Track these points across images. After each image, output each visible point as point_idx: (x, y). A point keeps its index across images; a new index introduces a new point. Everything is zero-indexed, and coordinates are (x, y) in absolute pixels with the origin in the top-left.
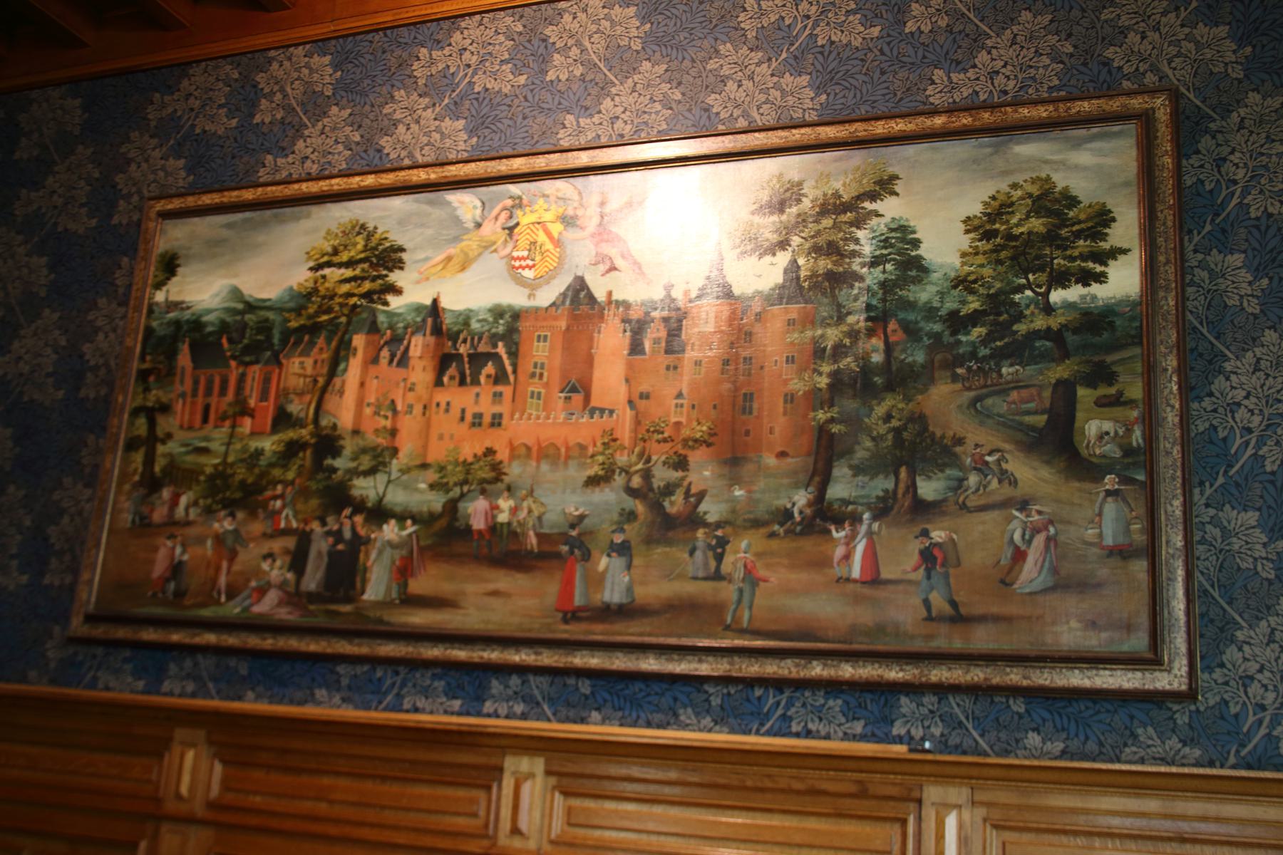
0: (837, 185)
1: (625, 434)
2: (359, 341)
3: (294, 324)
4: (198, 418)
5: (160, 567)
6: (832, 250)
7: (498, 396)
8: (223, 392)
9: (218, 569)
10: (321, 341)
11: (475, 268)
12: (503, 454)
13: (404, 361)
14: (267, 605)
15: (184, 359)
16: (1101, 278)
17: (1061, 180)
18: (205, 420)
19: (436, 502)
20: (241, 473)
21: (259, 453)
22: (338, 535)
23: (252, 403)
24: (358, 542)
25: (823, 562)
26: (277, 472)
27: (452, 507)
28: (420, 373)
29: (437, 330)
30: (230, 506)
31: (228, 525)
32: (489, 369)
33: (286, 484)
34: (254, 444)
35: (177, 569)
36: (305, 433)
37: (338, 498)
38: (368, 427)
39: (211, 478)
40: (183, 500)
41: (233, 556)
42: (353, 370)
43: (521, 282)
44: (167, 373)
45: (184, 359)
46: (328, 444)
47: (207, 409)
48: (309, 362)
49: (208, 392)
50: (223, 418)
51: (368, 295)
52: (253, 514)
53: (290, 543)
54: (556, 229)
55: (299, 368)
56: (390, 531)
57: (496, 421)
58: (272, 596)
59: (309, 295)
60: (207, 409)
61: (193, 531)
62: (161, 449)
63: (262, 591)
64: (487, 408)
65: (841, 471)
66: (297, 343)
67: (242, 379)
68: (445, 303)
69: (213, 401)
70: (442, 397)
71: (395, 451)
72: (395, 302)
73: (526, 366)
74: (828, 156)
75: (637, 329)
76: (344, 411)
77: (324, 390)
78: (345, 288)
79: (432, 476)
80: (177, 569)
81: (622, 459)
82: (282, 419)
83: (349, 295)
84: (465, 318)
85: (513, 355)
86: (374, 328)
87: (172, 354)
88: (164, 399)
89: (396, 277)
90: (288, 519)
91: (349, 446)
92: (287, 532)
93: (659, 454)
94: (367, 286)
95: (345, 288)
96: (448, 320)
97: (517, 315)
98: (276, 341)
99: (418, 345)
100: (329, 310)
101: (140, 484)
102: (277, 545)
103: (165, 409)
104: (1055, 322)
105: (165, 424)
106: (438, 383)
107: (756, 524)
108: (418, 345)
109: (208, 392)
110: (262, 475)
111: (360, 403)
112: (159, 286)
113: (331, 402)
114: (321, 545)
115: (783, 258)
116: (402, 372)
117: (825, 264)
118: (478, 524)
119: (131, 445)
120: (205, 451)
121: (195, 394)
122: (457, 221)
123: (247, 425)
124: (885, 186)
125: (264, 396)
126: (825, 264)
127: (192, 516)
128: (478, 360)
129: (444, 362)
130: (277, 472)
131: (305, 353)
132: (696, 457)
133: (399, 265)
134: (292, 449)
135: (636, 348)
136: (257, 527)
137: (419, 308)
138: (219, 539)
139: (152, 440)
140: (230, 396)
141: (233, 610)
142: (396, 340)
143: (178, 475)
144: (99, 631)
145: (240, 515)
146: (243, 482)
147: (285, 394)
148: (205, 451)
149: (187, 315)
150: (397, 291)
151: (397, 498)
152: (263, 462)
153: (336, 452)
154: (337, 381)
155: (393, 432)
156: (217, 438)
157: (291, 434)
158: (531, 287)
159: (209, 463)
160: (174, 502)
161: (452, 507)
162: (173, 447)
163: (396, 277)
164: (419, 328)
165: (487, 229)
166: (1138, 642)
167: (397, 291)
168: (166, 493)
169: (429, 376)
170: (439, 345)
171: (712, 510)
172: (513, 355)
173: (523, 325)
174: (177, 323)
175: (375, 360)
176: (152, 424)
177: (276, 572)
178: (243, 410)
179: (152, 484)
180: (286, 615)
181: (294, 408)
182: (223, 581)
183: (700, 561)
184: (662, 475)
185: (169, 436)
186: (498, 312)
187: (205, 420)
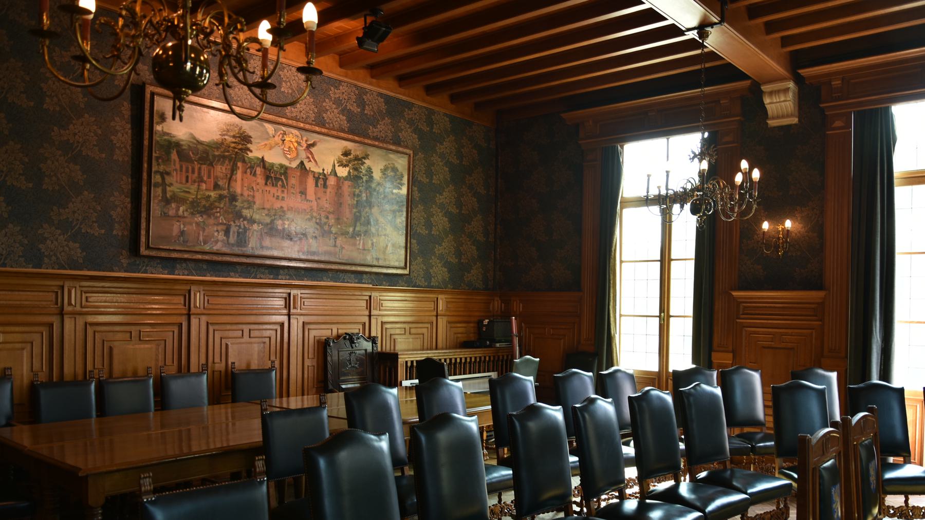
0: (358, 153)
1: (315, 208)
2: (239, 164)
3: (216, 153)
4: (184, 180)
5: (175, 232)
6: (356, 169)
7: (283, 191)
8: (193, 172)
9: (199, 234)
10: (227, 162)
11: (273, 150)
12: (285, 209)
13: (255, 175)
14: (218, 247)
15: (174, 156)
16: (400, 189)
17: (397, 165)
18: (187, 181)
19: (268, 220)
20: (204, 202)
21: (209, 196)
22: (239, 227)
23: (205, 178)
24: (245, 230)
25: (355, 245)
26: (217, 204)
27: (272, 222)
28: (260, 180)
29: (264, 167)
30: (201, 213)
31: (200, 219)
32: (280, 183)
33: (221, 208)
34: (207, 193)
35: (182, 233)
36: (225, 192)
37: (239, 215)
38: (246, 193)
39: (192, 203)
40: (181, 209)
41: (204, 230)
42: (239, 175)
43: (287, 158)
44: (167, 160)
45: (174, 156)
46: (233, 198)
47: (187, 177)
48: (224, 168)
49: (187, 171)
50: (195, 182)
51: (241, 149)
52: (209, 216)
53: (224, 227)
54: (296, 144)
55: (221, 170)
56: (255, 227)
57: (283, 199)
58: (220, 244)
59: (222, 143)
60: (187, 177)
61: (187, 220)
62: (168, 188)
63: (217, 242)
64: (279, 193)
65: (358, 224)
66: (219, 160)
67: (200, 169)
68: (266, 159)
69: (190, 175)
70: (268, 188)
71: (255, 203)
72: (250, 155)
73: (290, 184)
74: (357, 145)
75: (317, 179)
76: (238, 188)
77: (230, 179)
78: (233, 145)
79: (266, 212)
80: (182, 233)
81: (315, 214)
82: (216, 187)
83: (235, 148)
84: (272, 165)
85: (286, 180)
86: (244, 161)
87: (168, 153)
88: (168, 170)
89: (249, 146)
90: (222, 219)
91: (240, 199)
92: (222, 224)
93: (323, 215)
94: (240, 146)
95: (233, 145)
96: (267, 165)
97: (287, 168)
98: (211, 157)
99: (259, 170)
100: (228, 151)
101: (160, 201)
102: (220, 228)
103: (168, 174)
104: (394, 197)
105: (168, 180)
106: (266, 184)
107: (342, 234)
108: (259, 170)
109: (187, 171)
110: (211, 204)
111: (242, 186)
112: (158, 123)
113: (233, 184)
114: (234, 229)
115: (347, 169)
116: (254, 179)
117: (356, 173)
118: (280, 228)
119: (157, 185)
120: (189, 192)
121: (181, 171)
122: (267, 133)
123: (204, 186)
124: (366, 156)
125: (209, 177)
126: (356, 173)
127: (186, 214)
128: (278, 179)
129: (267, 178)
130: (217, 204)
131: (222, 164)
132: (331, 216)
133: (250, 142)
134: (221, 197)
135: (317, 185)
136: (211, 221)
137: (258, 158)
138: (198, 224)
139: (164, 184)
140: (196, 175)
141: (207, 248)
142: (252, 167)
143: (175, 198)
144: (153, 253)
145: (205, 217)
146: (204, 206)
147: (216, 178)
148: (189, 192)
149: (174, 140)
150: (251, 151)
151: (256, 217)
152: (211, 200)
153: (236, 200)
154: (234, 177)
155: (254, 197)
156: (193, 188)
157: (220, 192)
158: (290, 160)
159: (191, 197)
160: (178, 209)
161: (272, 222)
162: (172, 188)
163: (249, 146)
164: (259, 166)
165: (276, 138)
166: (403, 264)
167: (251, 151)
168: (173, 205)
169: (264, 182)
170: (265, 173)
171: (334, 230)
172: (286, 180)
173: (289, 172)
174: (170, 142)
175: (246, 172)
176: (163, 179)
177: (221, 236)
178: (201, 180)
179: (167, 201)
180: (225, 250)
181: (220, 183)
182: (201, 238)
183: (332, 241)
184: (324, 220)
185: (171, 184)
186: (282, 166)
187: (187, 181)
